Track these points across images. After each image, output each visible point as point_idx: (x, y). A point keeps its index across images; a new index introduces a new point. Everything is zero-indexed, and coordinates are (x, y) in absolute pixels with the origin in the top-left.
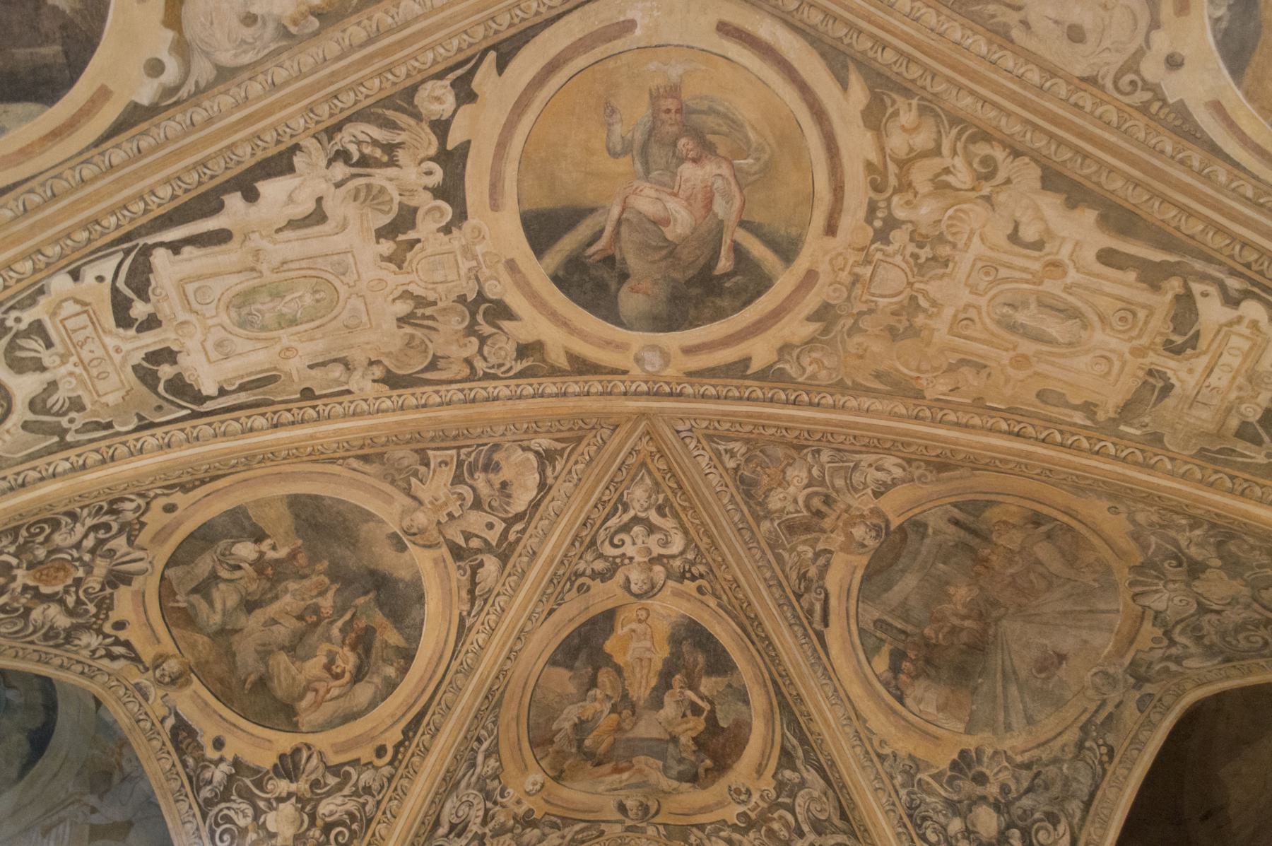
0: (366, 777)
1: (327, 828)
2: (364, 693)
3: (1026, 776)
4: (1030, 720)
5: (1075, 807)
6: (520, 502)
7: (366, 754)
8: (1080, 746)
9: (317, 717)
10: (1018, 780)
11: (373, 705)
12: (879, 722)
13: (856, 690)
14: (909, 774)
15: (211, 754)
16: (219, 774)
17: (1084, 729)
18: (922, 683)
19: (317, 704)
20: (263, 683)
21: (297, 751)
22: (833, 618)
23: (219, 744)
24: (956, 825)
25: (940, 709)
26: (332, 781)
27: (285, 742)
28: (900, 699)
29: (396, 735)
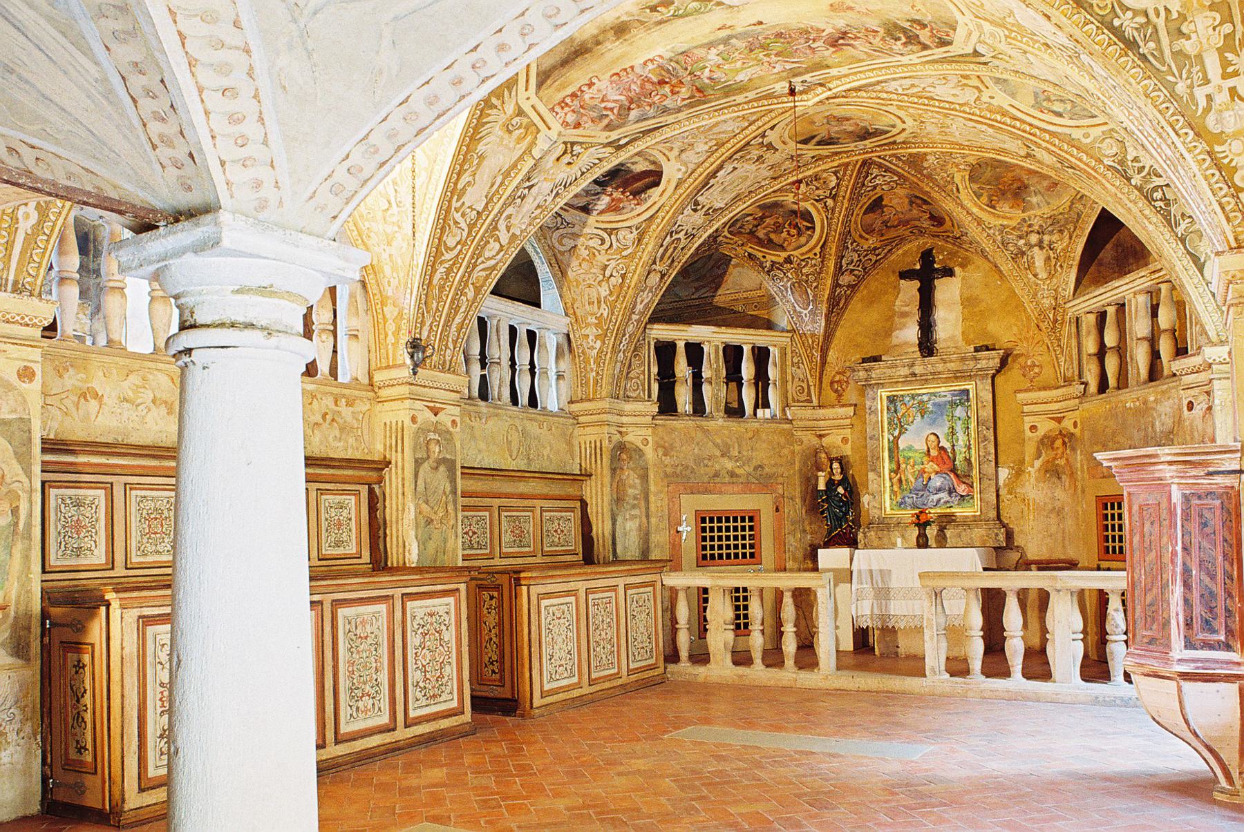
0: (814, 262)
1: (807, 276)
2: (803, 239)
3: (1049, 221)
4: (1048, 204)
5: (1071, 226)
6: (833, 184)
7: (811, 255)
8: (1070, 207)
9: (791, 248)
10: (1046, 223)
11: (807, 242)
12: (984, 216)
13: (975, 210)
14: (1001, 232)
15: (762, 259)
16: (768, 264)
17: (1072, 203)
18: (1001, 202)
19: (790, 244)
20: (770, 240)
21: (789, 256)
22: (961, 190)
23: (764, 257)
24: (1022, 242)
25: (1012, 207)
26: (804, 263)
27: (784, 255)
28: (994, 207)
29: (818, 250)
